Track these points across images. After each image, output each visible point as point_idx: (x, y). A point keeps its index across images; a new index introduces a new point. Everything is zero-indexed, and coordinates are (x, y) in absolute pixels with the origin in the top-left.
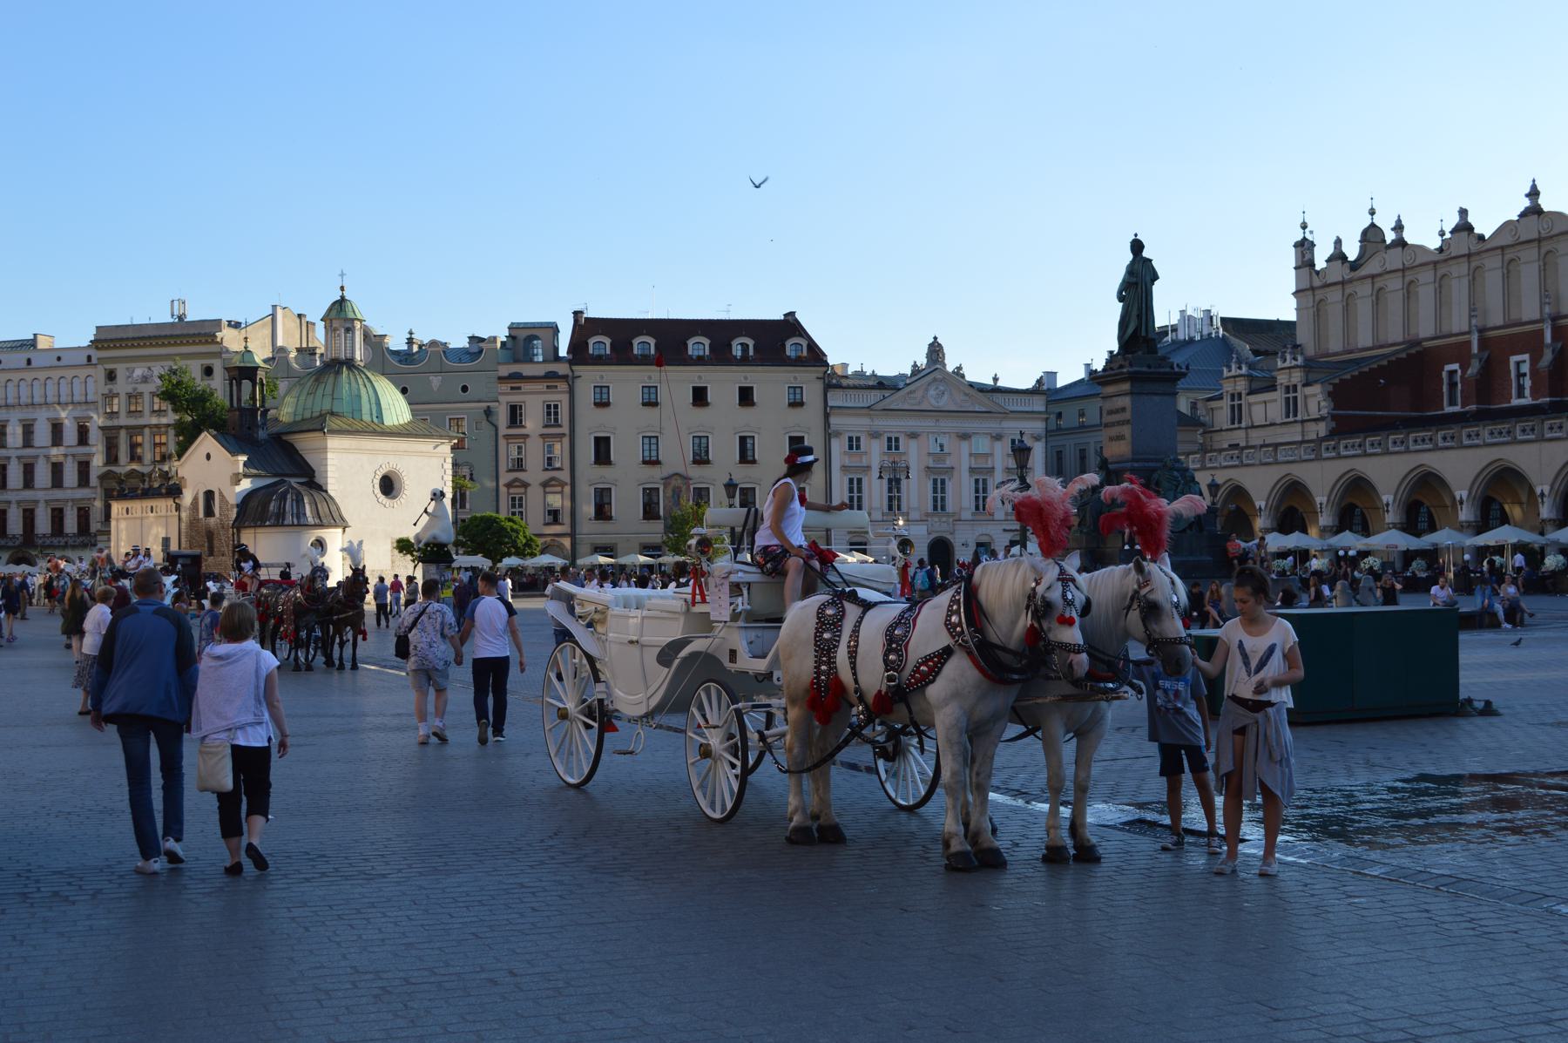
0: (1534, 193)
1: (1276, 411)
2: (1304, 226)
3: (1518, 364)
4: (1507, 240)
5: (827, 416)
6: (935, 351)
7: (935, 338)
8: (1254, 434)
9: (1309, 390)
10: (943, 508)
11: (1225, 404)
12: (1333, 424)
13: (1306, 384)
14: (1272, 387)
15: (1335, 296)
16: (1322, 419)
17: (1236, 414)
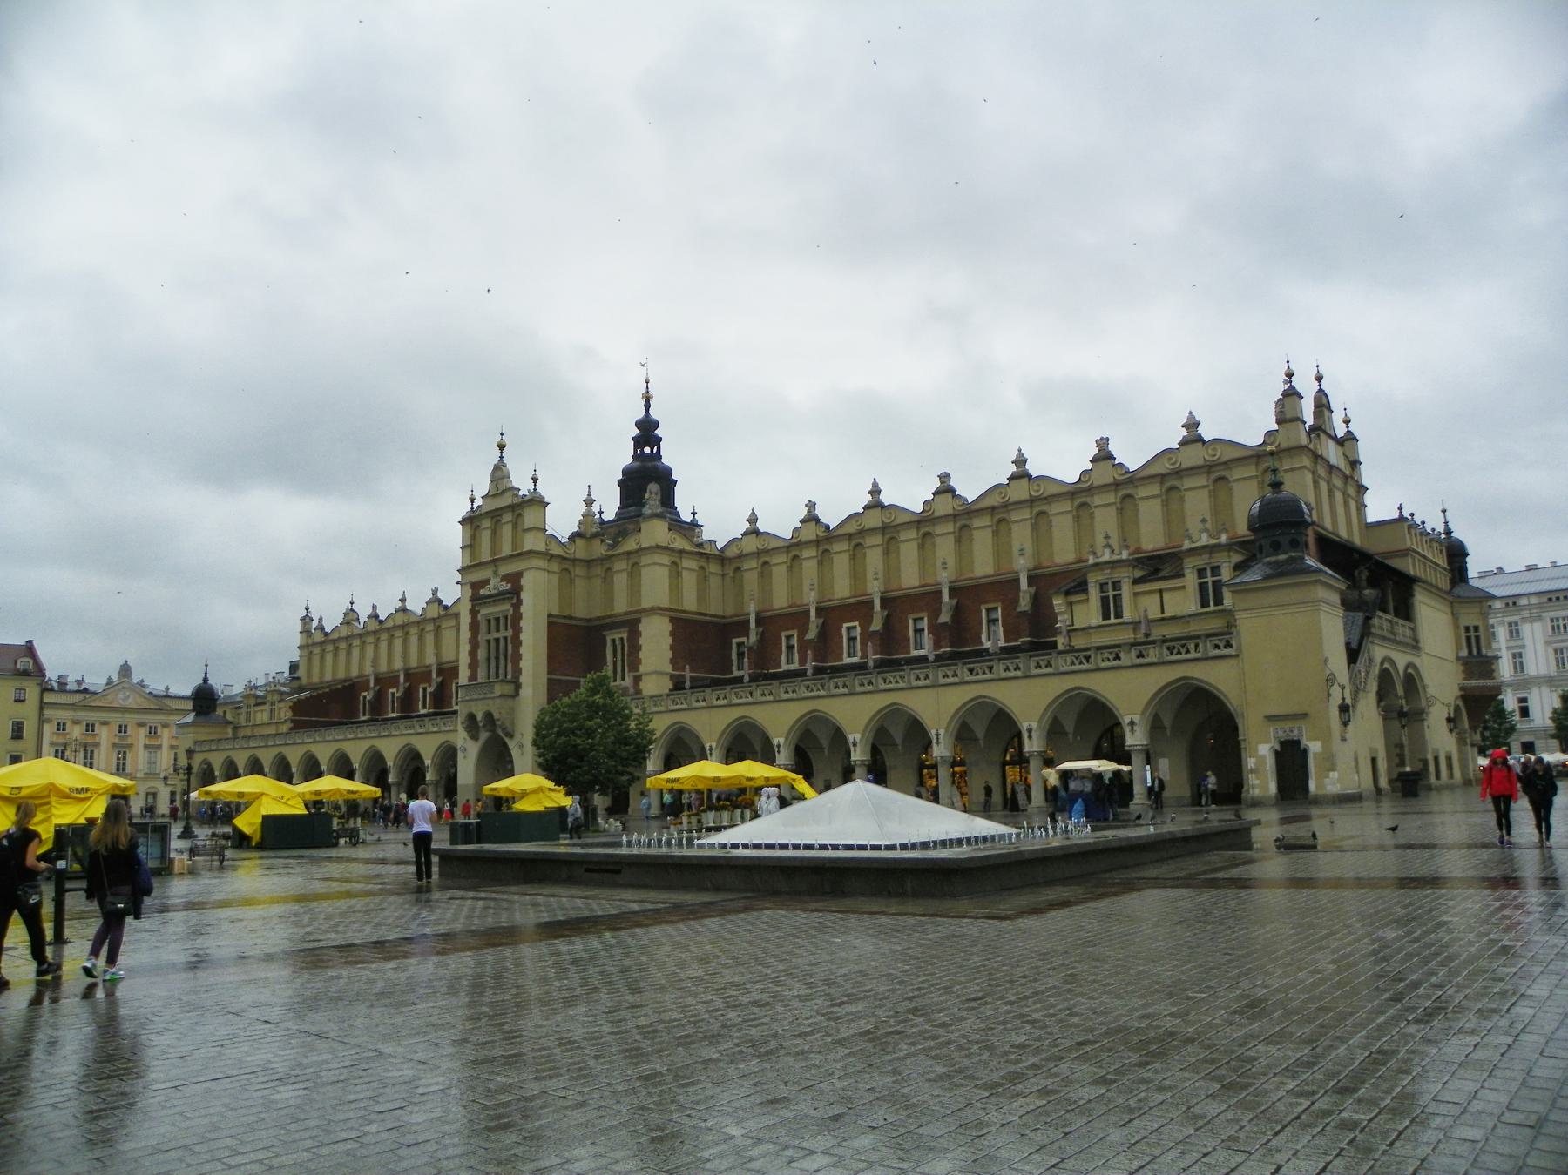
3: (393, 694)
4: (390, 624)
6: (125, 670)
9: (281, 705)
10: (124, 769)
13: (279, 702)
14: (264, 703)
15: (317, 650)
16: (286, 721)
17: (248, 714)
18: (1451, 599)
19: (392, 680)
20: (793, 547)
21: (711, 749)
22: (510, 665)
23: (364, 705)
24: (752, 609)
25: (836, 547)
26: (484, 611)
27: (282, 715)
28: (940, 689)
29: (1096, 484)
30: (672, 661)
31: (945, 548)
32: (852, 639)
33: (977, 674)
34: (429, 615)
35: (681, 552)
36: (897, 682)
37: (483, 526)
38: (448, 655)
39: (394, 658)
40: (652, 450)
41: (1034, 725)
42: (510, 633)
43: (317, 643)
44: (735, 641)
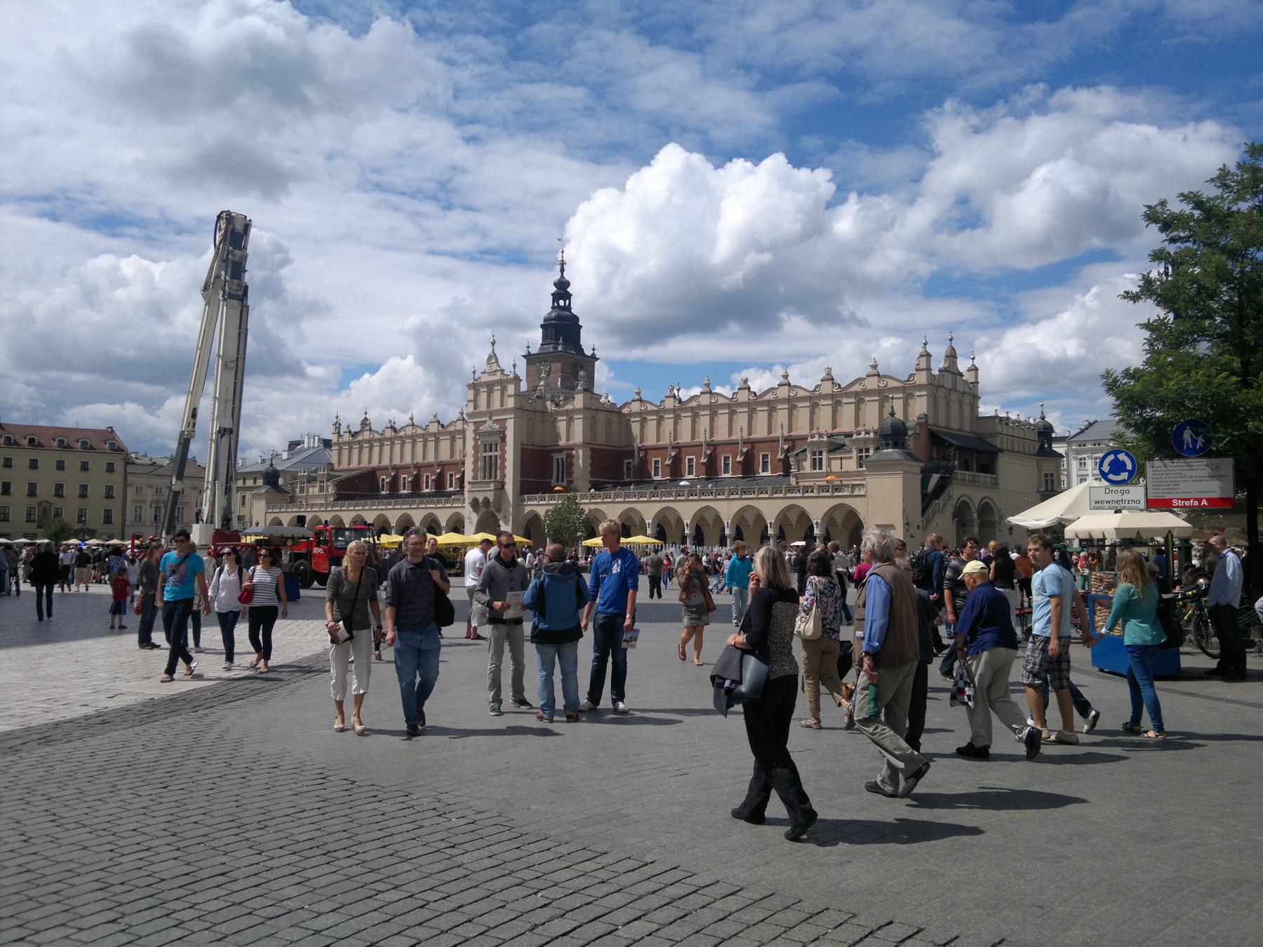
1: (316, 490)
2: (337, 417)
3: (404, 478)
4: (402, 433)
5: (126, 477)
13: (327, 481)
14: (315, 479)
18: (1038, 458)
22: (498, 472)
26: (483, 439)
27: (330, 488)
28: (730, 502)
29: (823, 393)
31: (742, 419)
35: (597, 410)
38: (445, 456)
39: (406, 456)
40: (565, 303)
41: (773, 521)
42: (498, 453)
44: (626, 461)
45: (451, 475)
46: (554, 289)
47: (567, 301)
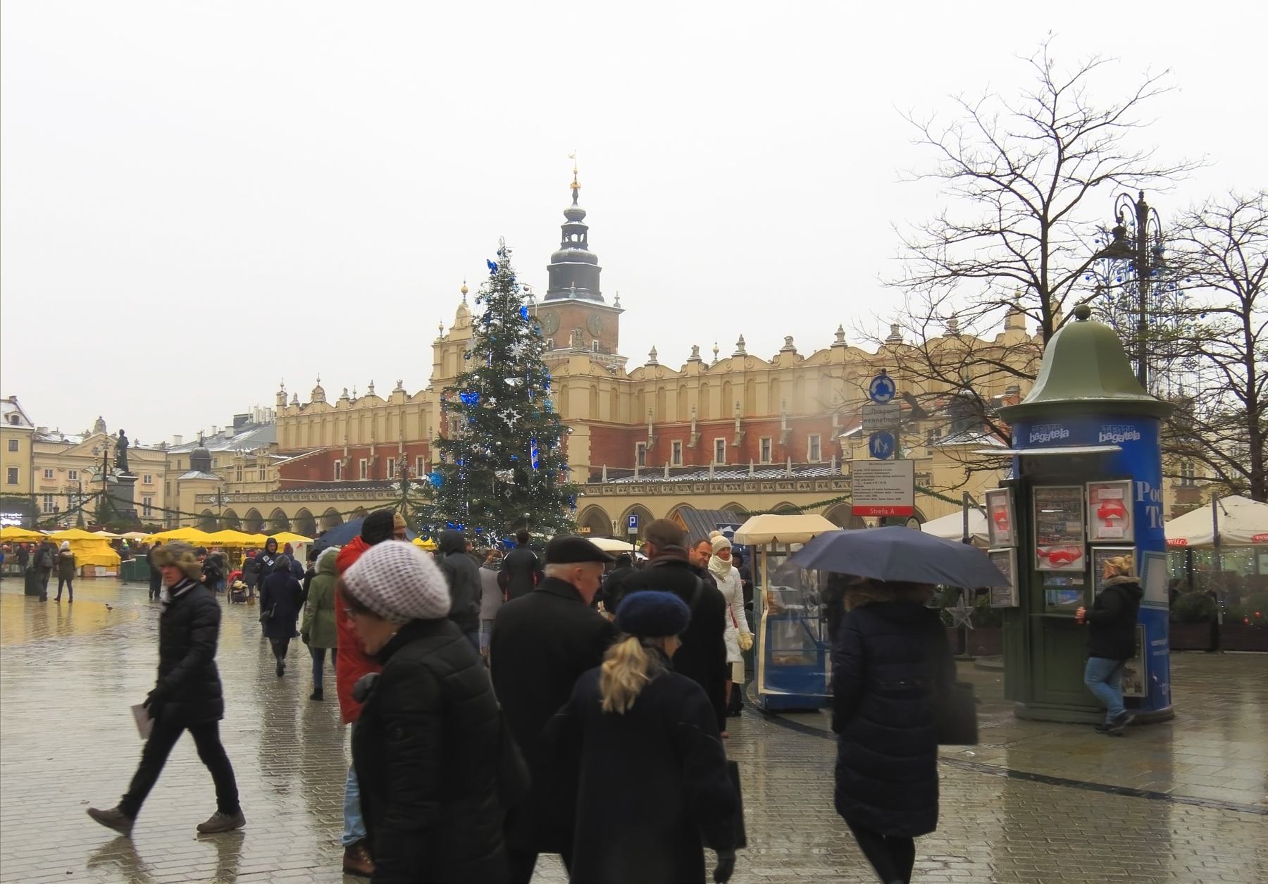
0: (372, 387)
1: (256, 477)
3: (364, 463)
4: (359, 406)
5: (32, 458)
7: (101, 417)
8: (247, 486)
9: (270, 468)
11: (235, 470)
12: (280, 485)
13: (269, 465)
14: (254, 465)
16: (274, 482)
17: (239, 475)
19: (364, 452)
20: (682, 379)
21: (615, 524)
23: (338, 470)
24: (650, 420)
25: (712, 382)
27: (271, 475)
28: (762, 496)
30: (590, 458)
32: (720, 450)
33: (784, 488)
34: (395, 402)
35: (598, 378)
36: (736, 489)
37: (451, 351)
39: (364, 434)
43: (293, 416)
44: (638, 443)
45: (420, 459)
46: (564, 220)
47: (582, 235)
